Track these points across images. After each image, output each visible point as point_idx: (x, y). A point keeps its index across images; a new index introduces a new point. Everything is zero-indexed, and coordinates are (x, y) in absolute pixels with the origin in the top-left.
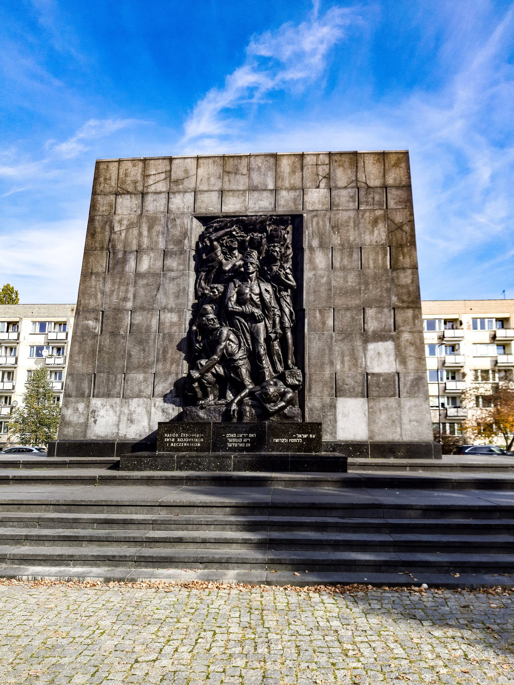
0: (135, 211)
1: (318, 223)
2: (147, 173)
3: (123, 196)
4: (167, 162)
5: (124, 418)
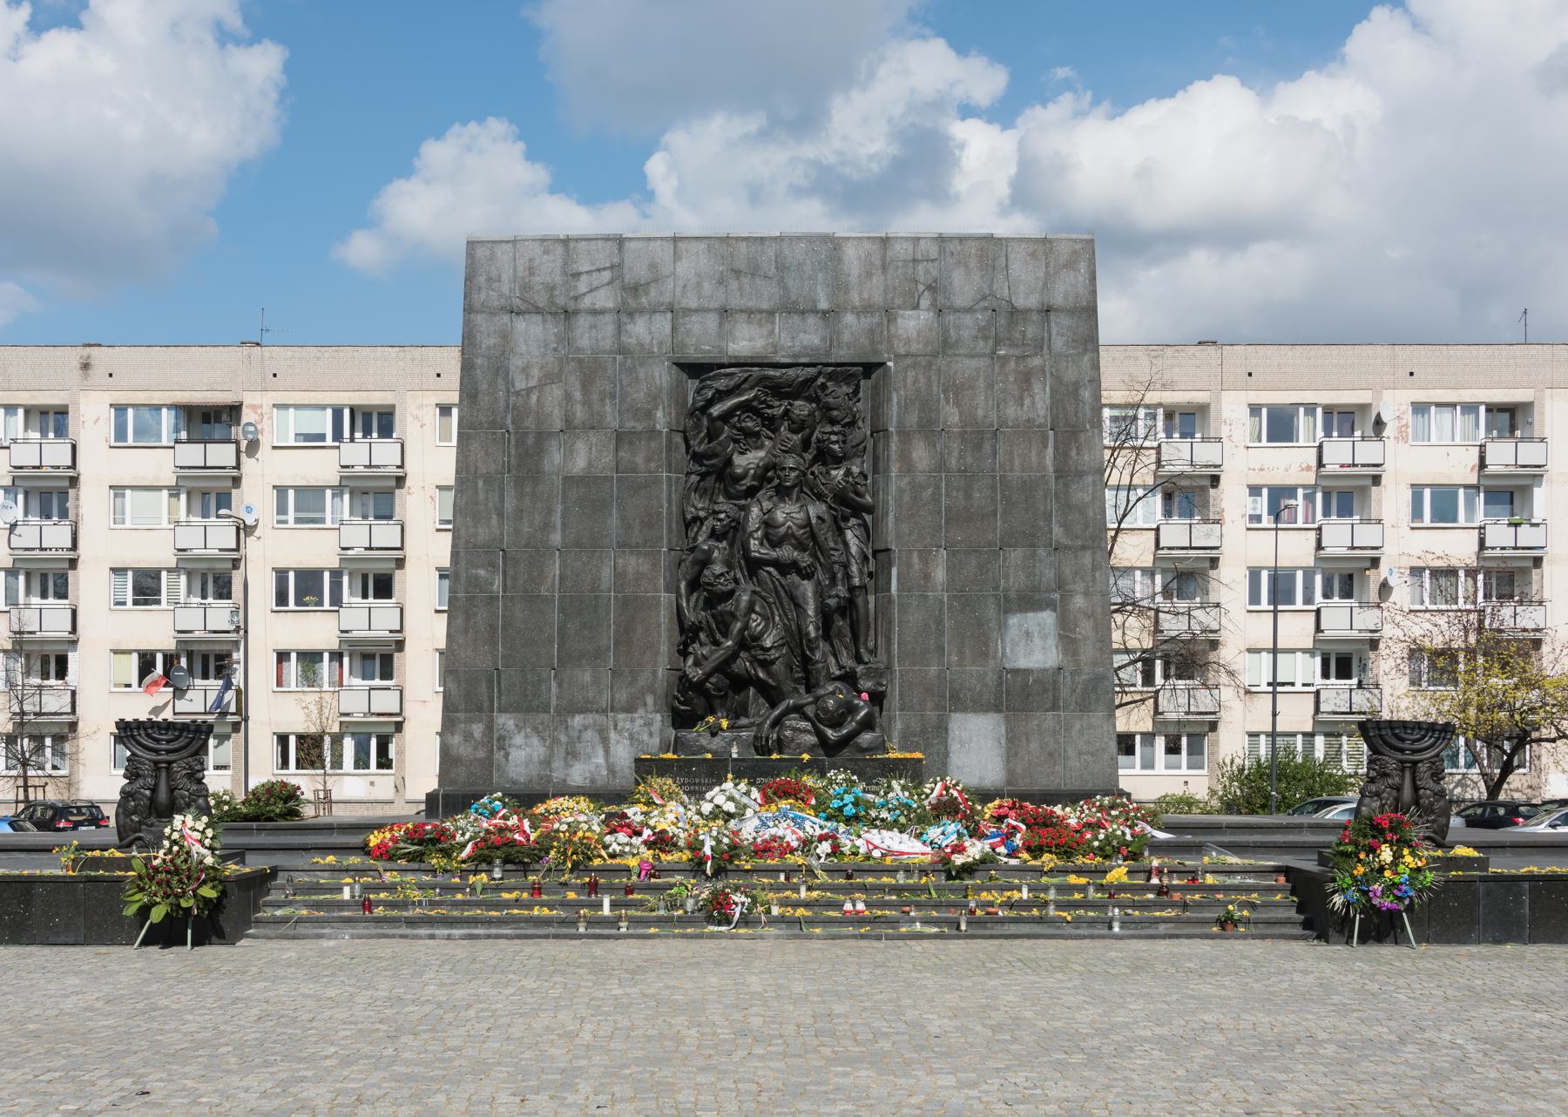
0: (555, 349)
1: (916, 381)
2: (575, 268)
3: (527, 316)
4: (614, 246)
5: (560, 752)
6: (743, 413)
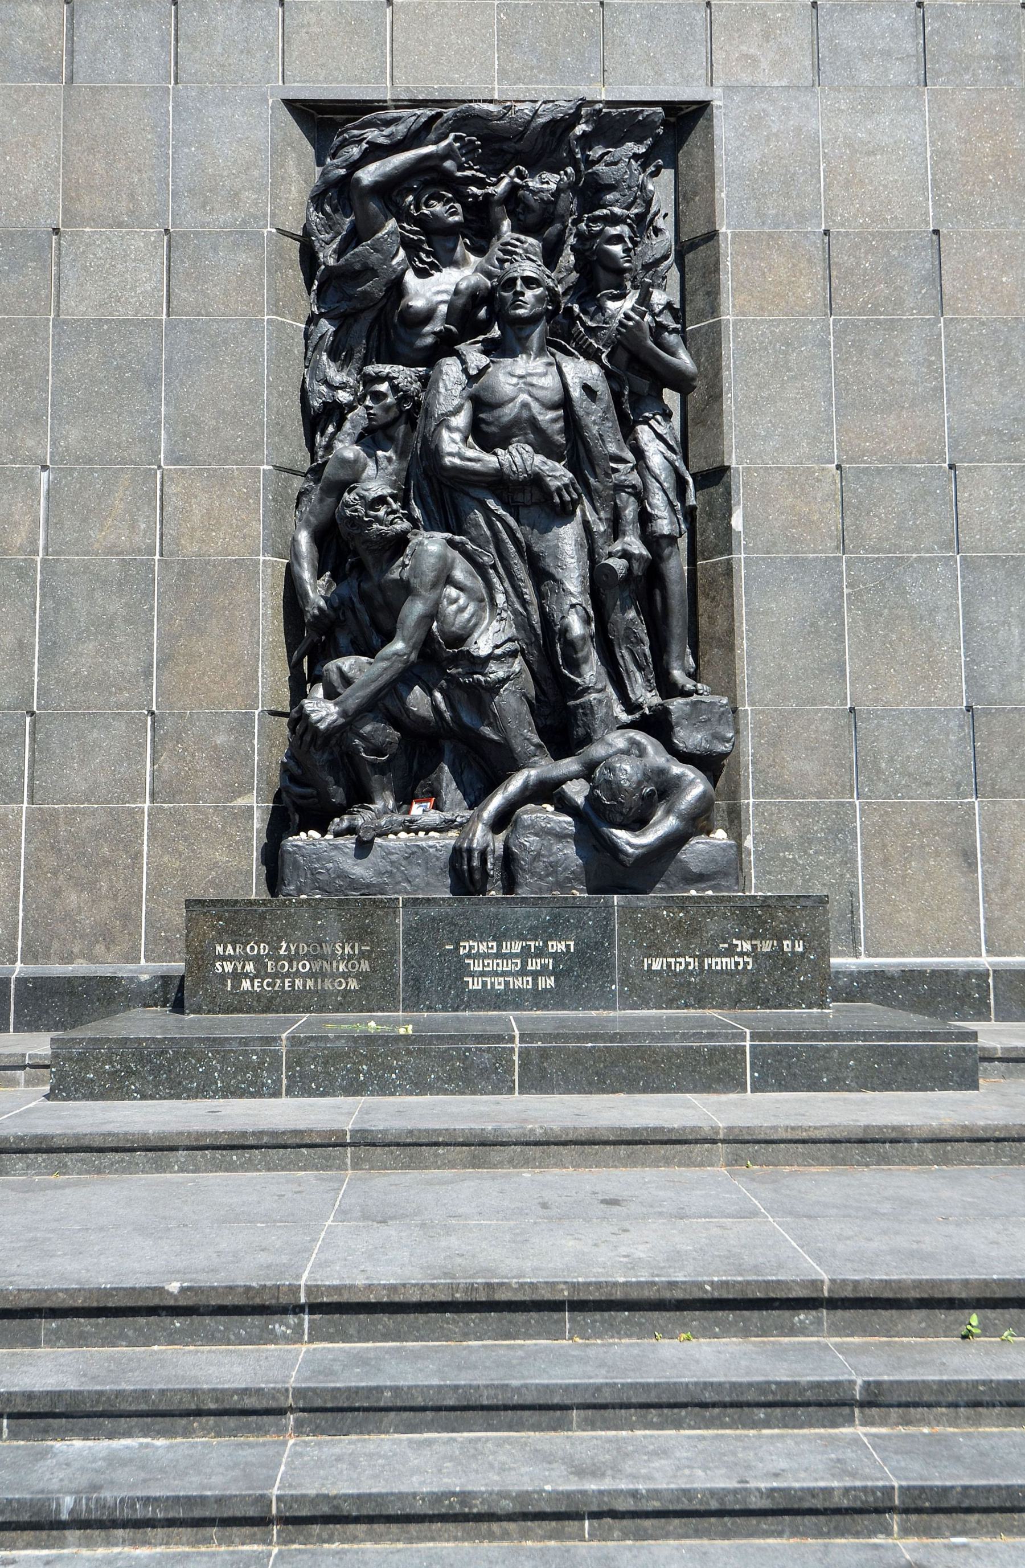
6: (426, 185)
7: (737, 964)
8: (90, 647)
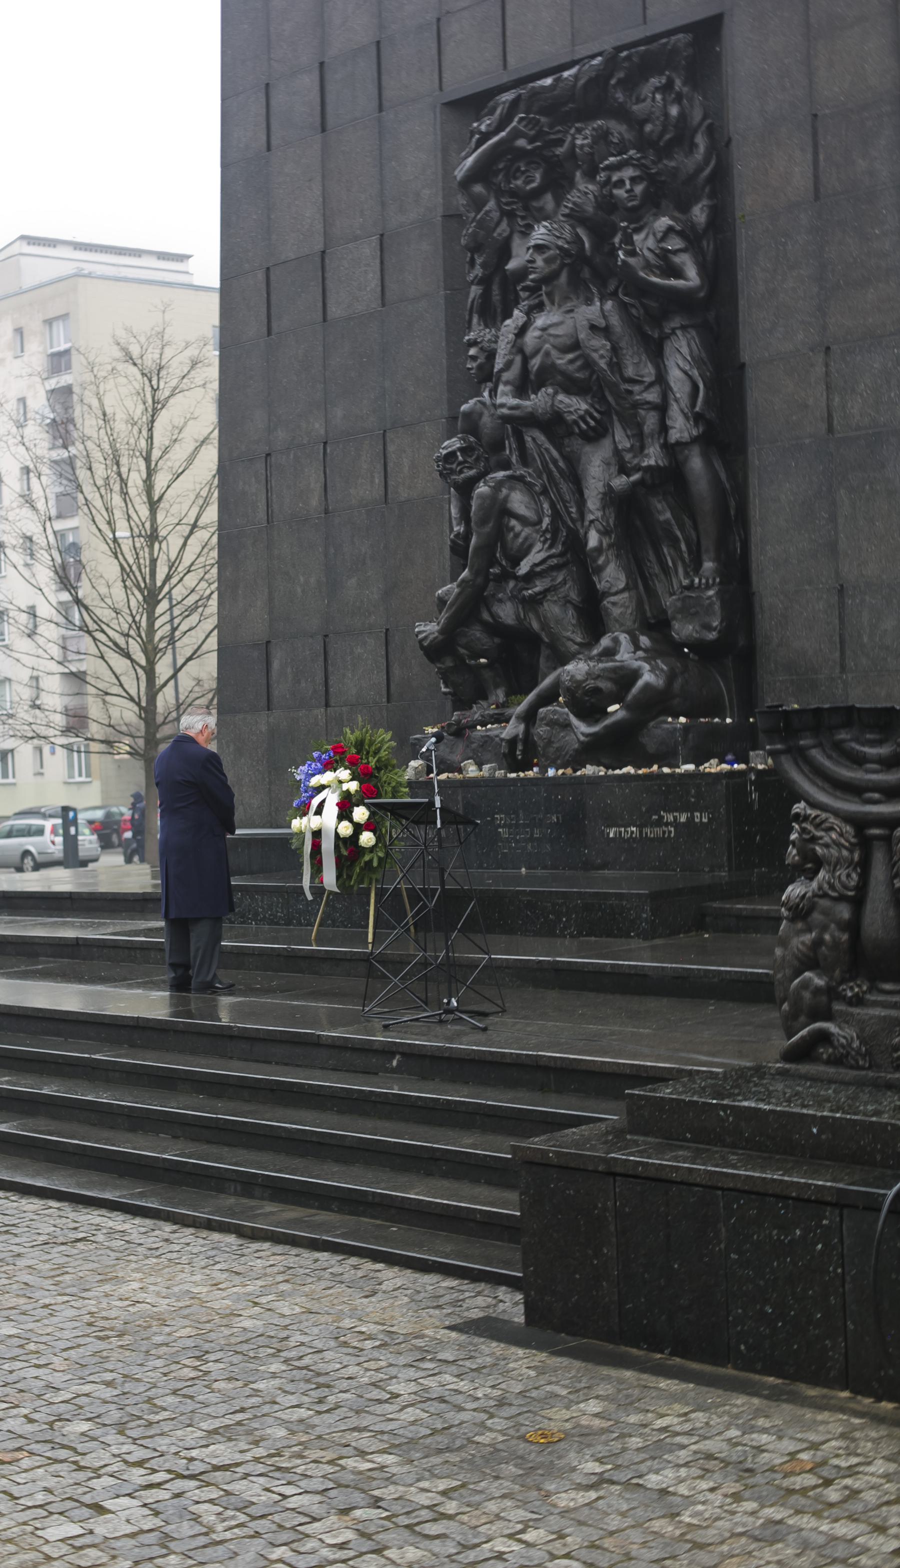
7: (664, 832)
8: (353, 581)
